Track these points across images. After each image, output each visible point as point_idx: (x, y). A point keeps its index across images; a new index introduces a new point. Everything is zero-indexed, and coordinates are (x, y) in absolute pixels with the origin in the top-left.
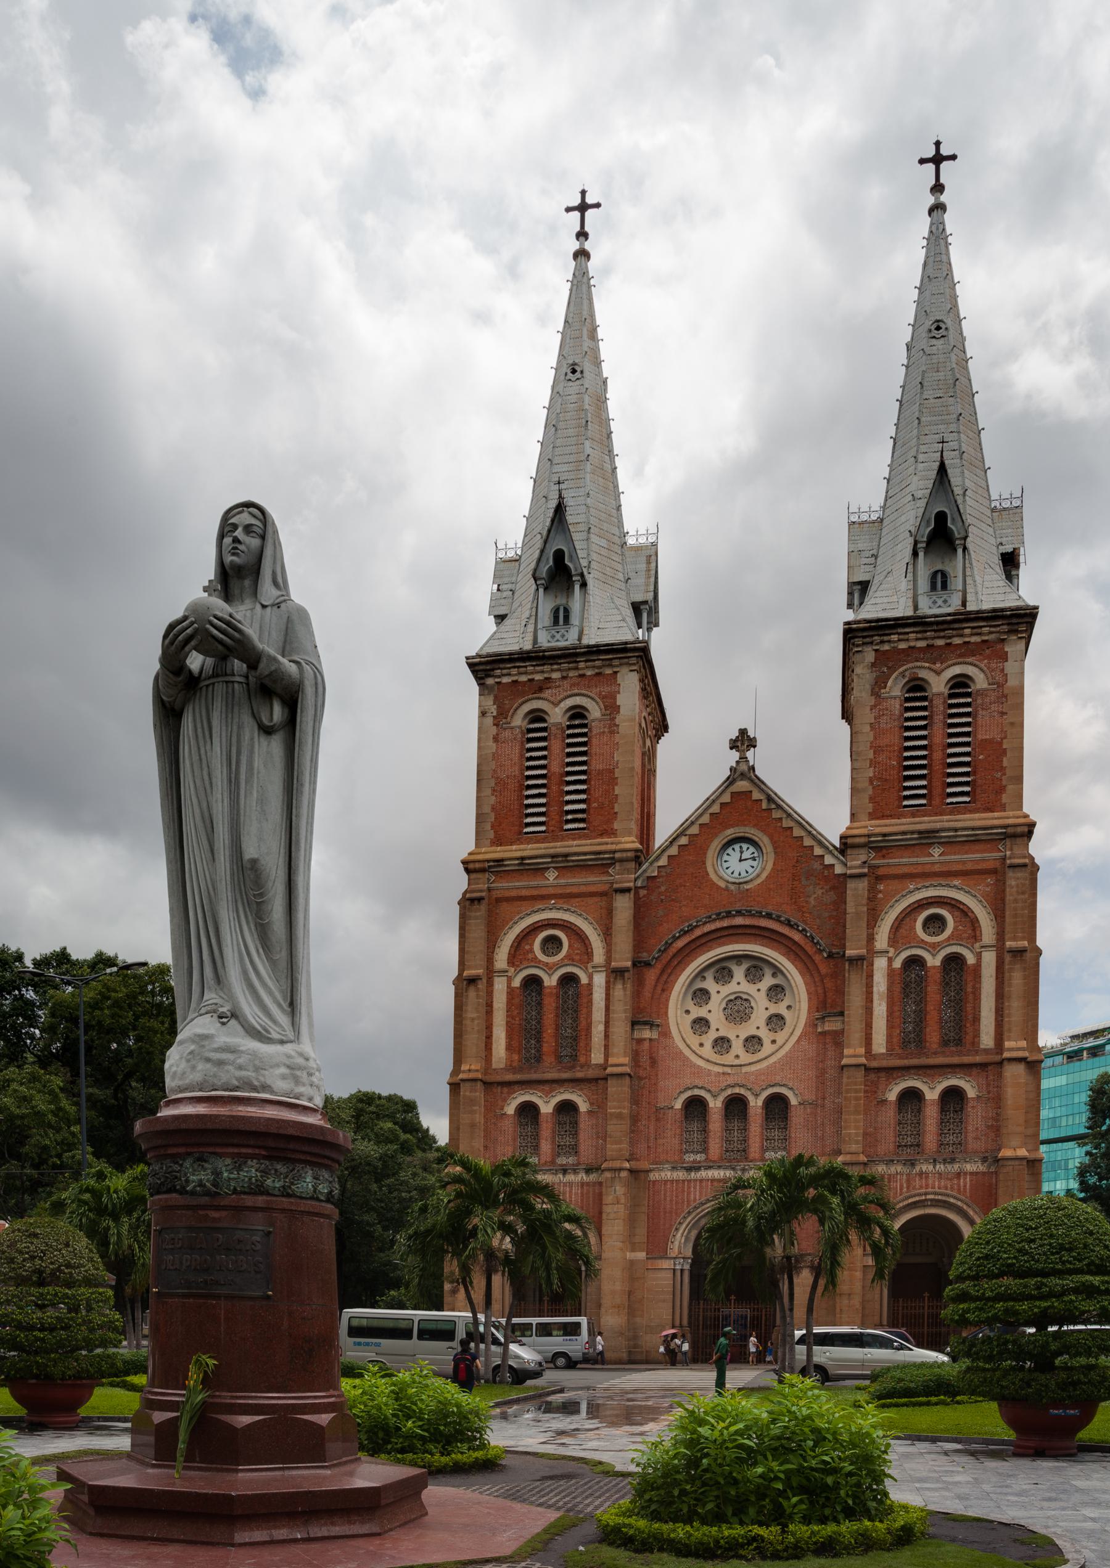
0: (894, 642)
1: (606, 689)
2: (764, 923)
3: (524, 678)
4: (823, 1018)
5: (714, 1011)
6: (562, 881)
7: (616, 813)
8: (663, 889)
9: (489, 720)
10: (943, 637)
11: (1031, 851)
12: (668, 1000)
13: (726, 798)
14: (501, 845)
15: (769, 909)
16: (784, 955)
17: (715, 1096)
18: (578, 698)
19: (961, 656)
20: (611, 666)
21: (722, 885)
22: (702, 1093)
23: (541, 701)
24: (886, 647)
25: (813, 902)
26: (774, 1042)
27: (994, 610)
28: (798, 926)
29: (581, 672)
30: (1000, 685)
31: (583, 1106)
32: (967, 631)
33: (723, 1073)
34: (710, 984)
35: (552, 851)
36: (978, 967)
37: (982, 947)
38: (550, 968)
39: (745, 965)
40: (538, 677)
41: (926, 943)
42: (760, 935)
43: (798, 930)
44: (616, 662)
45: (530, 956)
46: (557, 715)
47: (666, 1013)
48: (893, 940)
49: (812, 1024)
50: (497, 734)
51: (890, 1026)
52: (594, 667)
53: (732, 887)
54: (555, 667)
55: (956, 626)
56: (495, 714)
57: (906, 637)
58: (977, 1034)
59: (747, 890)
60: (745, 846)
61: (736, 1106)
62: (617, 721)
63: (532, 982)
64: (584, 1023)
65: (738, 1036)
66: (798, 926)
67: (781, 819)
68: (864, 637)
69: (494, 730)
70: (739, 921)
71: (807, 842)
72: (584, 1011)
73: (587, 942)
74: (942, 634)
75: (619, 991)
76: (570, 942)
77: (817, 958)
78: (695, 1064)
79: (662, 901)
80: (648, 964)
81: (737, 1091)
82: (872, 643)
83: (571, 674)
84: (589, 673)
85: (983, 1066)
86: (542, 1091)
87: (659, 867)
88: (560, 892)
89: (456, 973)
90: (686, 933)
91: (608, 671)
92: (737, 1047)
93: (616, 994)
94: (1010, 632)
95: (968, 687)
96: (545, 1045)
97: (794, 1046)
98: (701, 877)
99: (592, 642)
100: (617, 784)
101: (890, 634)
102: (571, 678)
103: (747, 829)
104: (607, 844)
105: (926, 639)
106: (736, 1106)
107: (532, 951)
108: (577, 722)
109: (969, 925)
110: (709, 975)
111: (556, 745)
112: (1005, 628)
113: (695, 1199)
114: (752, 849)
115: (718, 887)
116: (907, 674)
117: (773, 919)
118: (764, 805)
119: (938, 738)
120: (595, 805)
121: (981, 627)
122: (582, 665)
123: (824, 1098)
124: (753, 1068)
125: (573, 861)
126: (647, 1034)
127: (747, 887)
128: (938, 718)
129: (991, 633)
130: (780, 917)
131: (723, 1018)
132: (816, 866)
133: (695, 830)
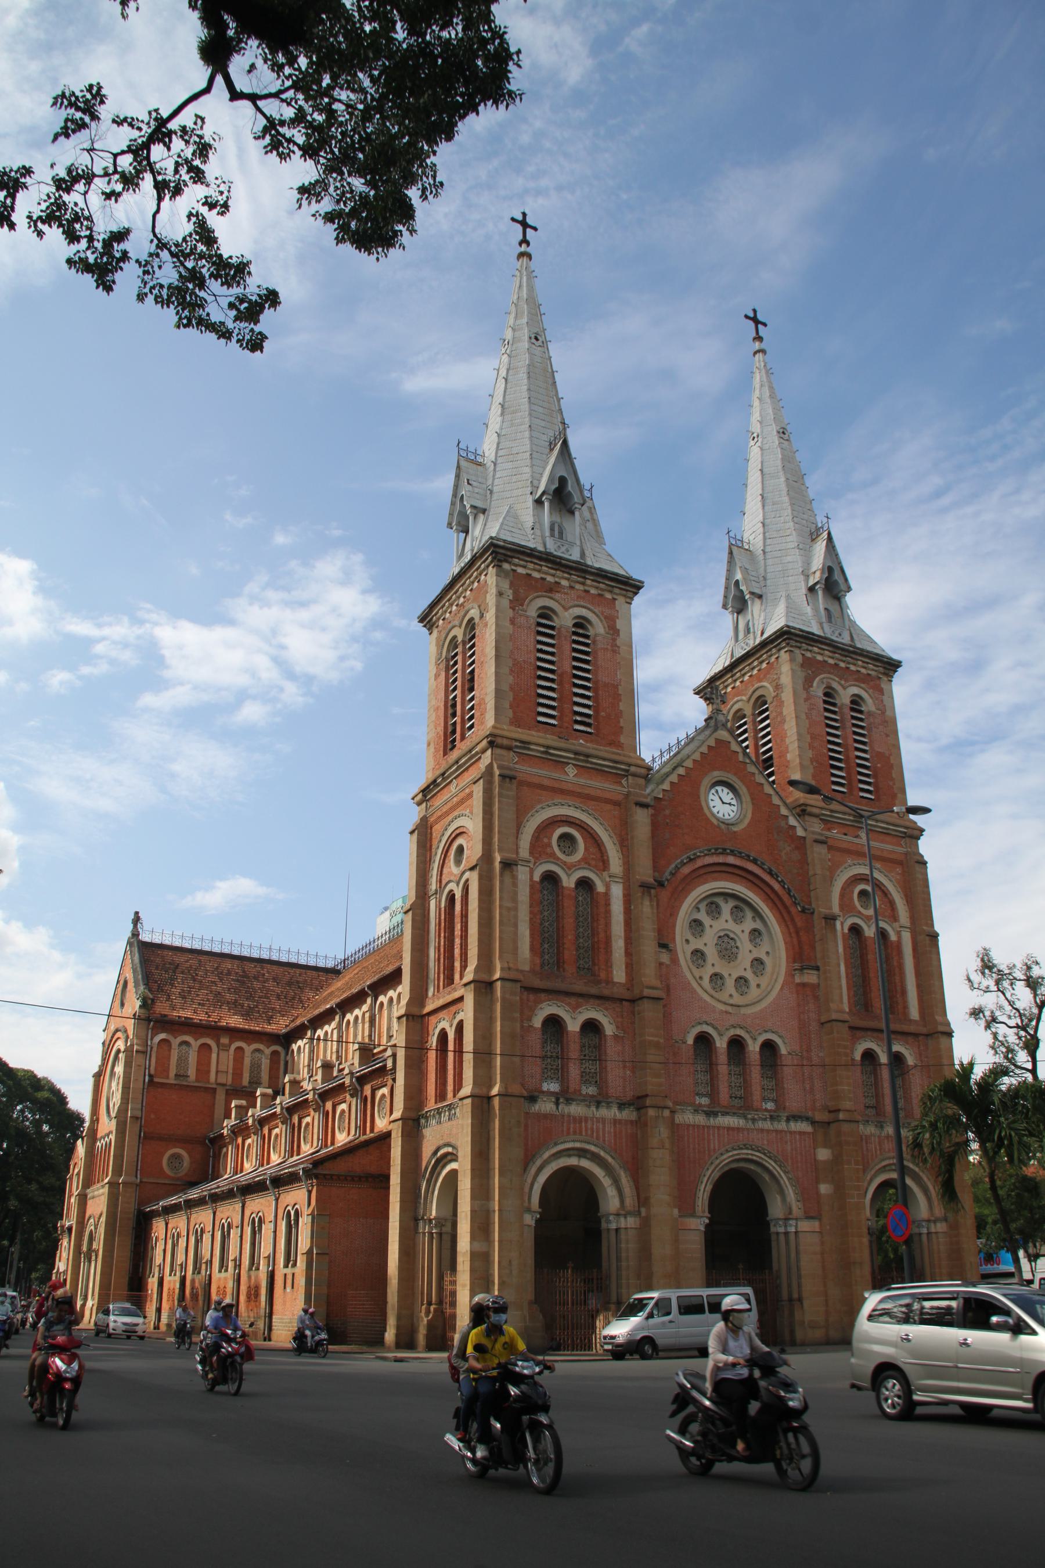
0: (815, 653)
1: (607, 612)
2: (751, 867)
3: (536, 575)
4: (802, 969)
5: (708, 942)
6: (582, 781)
7: (622, 727)
8: (667, 812)
9: (505, 603)
10: (844, 662)
11: (922, 851)
12: (674, 926)
13: (712, 742)
14: (519, 727)
15: (753, 855)
16: (763, 901)
17: (721, 1035)
18: (584, 610)
19: (856, 680)
20: (611, 592)
21: (715, 822)
22: (709, 1030)
23: (552, 601)
24: (808, 655)
25: (784, 857)
26: (758, 986)
27: (877, 654)
28: (778, 876)
29: (587, 588)
30: (883, 713)
31: (609, 1029)
32: (860, 663)
33: (726, 1012)
34: (702, 916)
35: (572, 747)
36: (899, 945)
37: (901, 927)
38: (569, 868)
39: (732, 903)
40: (549, 579)
41: (863, 914)
42: (745, 878)
43: (777, 880)
44: (617, 591)
45: (549, 850)
46: (565, 619)
47: (674, 939)
48: (842, 907)
49: (790, 975)
50: (514, 618)
51: (849, 989)
52: (597, 588)
53: (723, 826)
54: (566, 575)
55: (854, 656)
56: (511, 598)
57: (822, 652)
58: (906, 1007)
59: (735, 832)
60: (726, 790)
61: (737, 1044)
62: (618, 643)
63: (550, 878)
64: (602, 935)
65: (730, 975)
66: (778, 876)
67: (754, 774)
68: (796, 641)
69: (510, 613)
70: (731, 860)
71: (776, 800)
72: (602, 921)
73: (602, 848)
74: (844, 659)
75: (646, 908)
76: (585, 845)
77: (792, 909)
78: (701, 999)
79: (667, 823)
80: (661, 884)
81: (738, 1033)
82: (799, 648)
83: (578, 586)
84: (593, 591)
85: (916, 1035)
86: (569, 1004)
87: (664, 790)
88: (580, 791)
89: (480, 854)
90: (691, 860)
91: (608, 596)
92: (730, 983)
93: (644, 910)
94: (885, 674)
95: (861, 706)
96: (566, 952)
97: (778, 994)
98: (698, 810)
99: (597, 565)
100: (620, 700)
101: (813, 646)
102: (577, 590)
103: (730, 776)
104: (620, 755)
105: (833, 658)
106: (737, 1044)
107: (549, 845)
108: (581, 631)
109: (888, 905)
110: (703, 907)
111: (567, 647)
112: (881, 669)
113: (714, 1147)
114: (731, 795)
115: (712, 823)
116: (825, 680)
117: (758, 865)
118: (741, 758)
119: (850, 742)
120: (603, 714)
121: (868, 663)
122: (588, 582)
123: (809, 1050)
124: (749, 1011)
125: (592, 763)
126: (665, 958)
127: (735, 829)
128: (849, 725)
129: (873, 670)
130: (764, 864)
131: (716, 953)
132: (783, 823)
133: (689, 764)
